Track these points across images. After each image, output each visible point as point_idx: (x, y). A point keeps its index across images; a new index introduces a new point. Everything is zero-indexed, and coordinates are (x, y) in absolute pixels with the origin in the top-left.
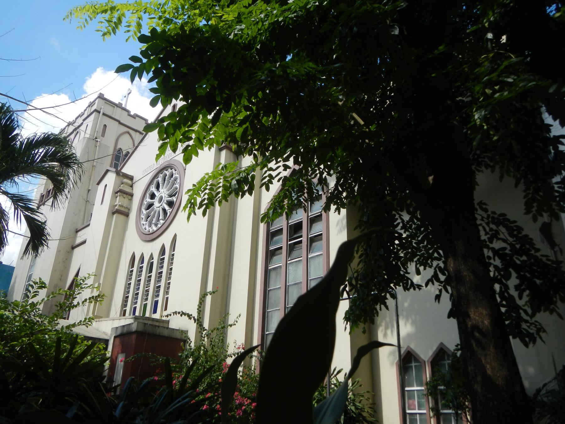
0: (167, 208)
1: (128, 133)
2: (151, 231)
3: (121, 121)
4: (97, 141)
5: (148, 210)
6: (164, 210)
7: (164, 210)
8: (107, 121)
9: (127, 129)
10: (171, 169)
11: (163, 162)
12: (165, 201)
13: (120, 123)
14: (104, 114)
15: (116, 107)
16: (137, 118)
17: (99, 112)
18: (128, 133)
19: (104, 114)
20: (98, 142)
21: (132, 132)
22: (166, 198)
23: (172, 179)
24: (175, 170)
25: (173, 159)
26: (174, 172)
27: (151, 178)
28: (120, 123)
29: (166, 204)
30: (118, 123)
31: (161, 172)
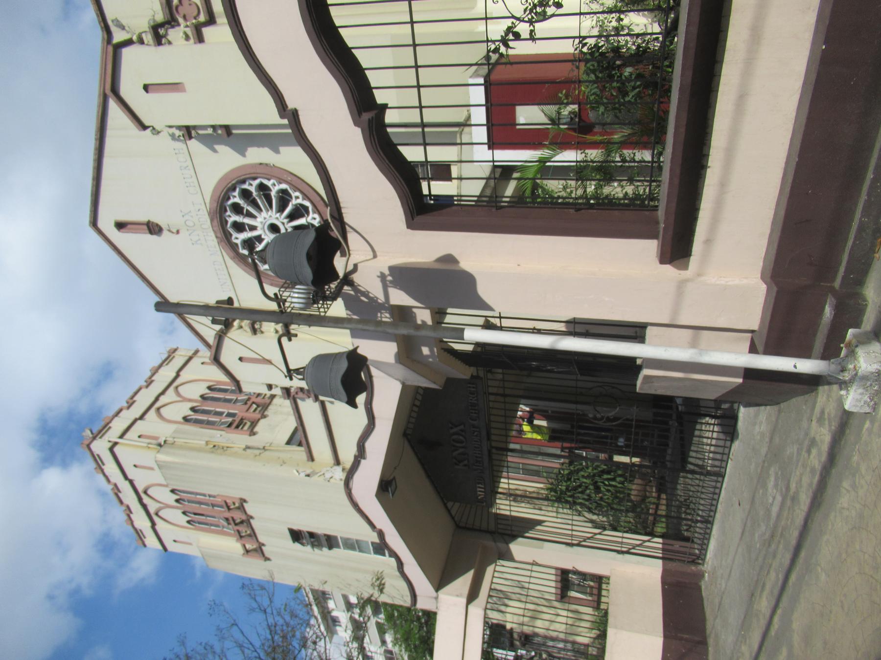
3: (138, 416)
4: (165, 441)
6: (292, 217)
7: (292, 217)
8: (132, 434)
12: (278, 215)
13: (141, 417)
14: (121, 437)
15: (110, 425)
16: (135, 399)
17: (116, 444)
20: (167, 439)
21: (158, 405)
28: (141, 417)
30: (139, 422)
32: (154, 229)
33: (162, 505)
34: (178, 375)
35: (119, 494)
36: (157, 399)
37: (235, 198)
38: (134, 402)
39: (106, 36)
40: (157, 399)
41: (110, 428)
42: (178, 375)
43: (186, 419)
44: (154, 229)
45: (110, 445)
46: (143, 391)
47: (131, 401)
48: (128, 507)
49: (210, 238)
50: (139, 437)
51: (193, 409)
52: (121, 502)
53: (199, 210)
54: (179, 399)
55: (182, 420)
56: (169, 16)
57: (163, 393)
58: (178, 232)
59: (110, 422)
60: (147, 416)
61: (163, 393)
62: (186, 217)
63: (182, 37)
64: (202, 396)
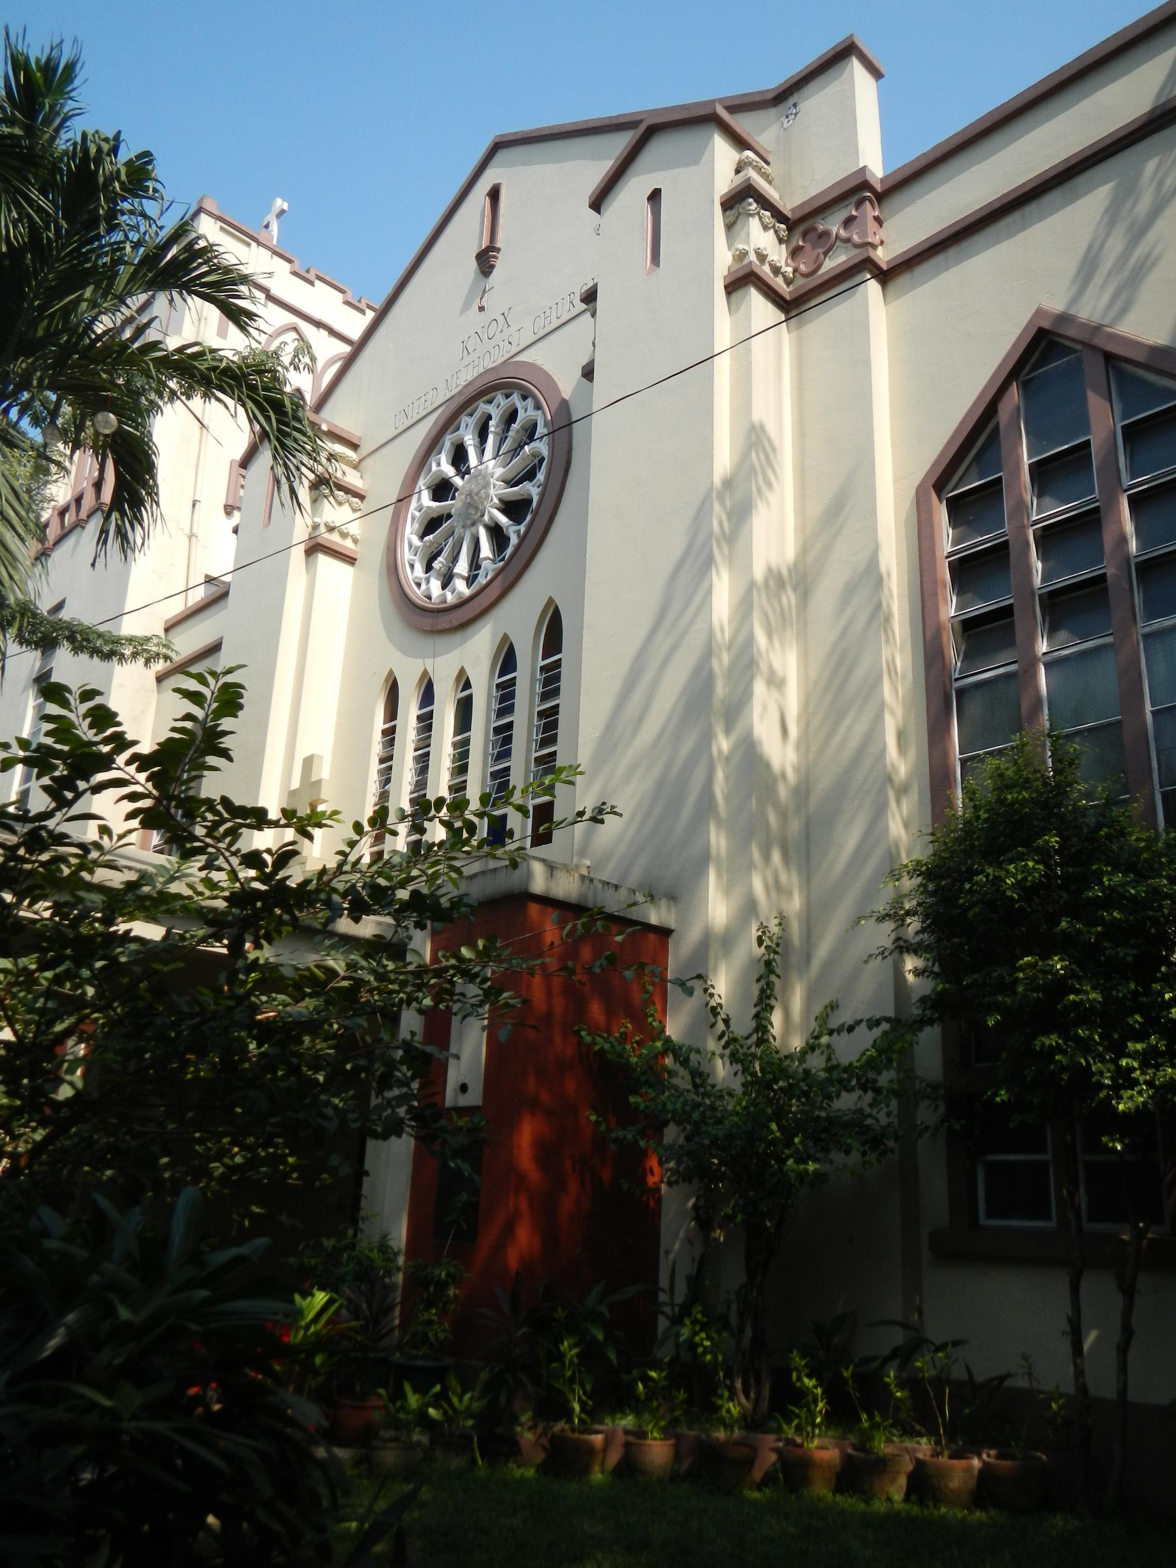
0: (503, 519)
1: (295, 329)
2: (450, 598)
3: (275, 292)
5: (431, 536)
6: (496, 532)
9: (292, 319)
10: (507, 396)
11: (475, 375)
12: (496, 501)
15: (254, 244)
18: (295, 329)
21: (305, 327)
22: (497, 491)
23: (515, 426)
24: (524, 398)
25: (518, 359)
26: (519, 404)
27: (434, 433)
29: (498, 509)
31: (468, 411)
32: (486, 260)
36: (318, 324)
37: (496, 410)
38: (312, 283)
39: (770, 96)
40: (318, 324)
41: (249, 245)
44: (486, 260)
46: (339, 296)
47: (311, 276)
49: (466, 375)
53: (510, 343)
56: (798, 215)
57: (333, 332)
58: (481, 309)
59: (259, 243)
61: (333, 332)
62: (501, 319)
63: (765, 249)
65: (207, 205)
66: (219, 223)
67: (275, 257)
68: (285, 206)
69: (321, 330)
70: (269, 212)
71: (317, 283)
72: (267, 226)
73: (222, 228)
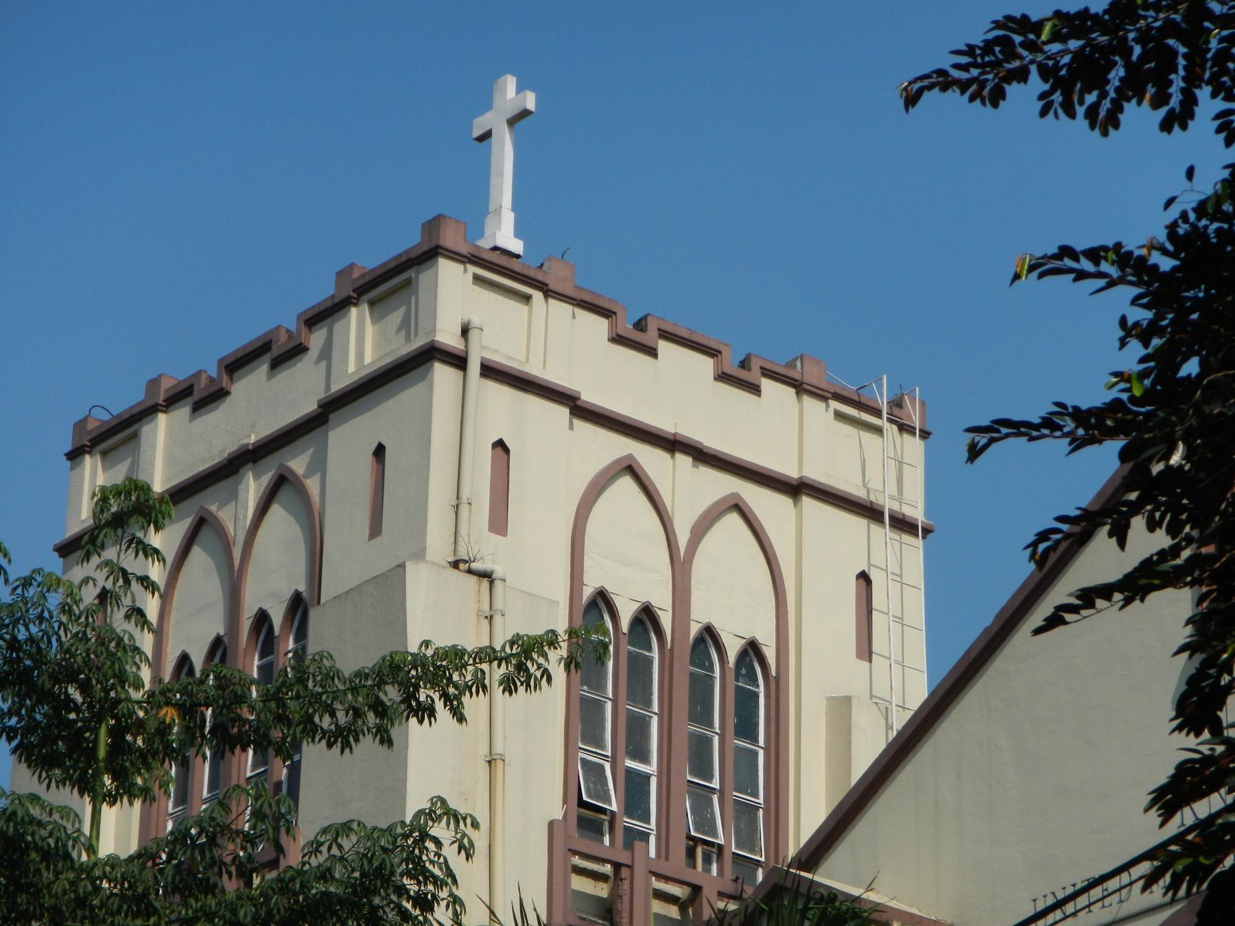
3: (590, 396)
14: (490, 371)
15: (537, 296)
17: (459, 361)
19: (490, 371)
21: (651, 459)
30: (564, 412)
33: (237, 553)
34: (795, 489)
35: (267, 358)
36: (672, 444)
38: (652, 352)
40: (672, 444)
41: (527, 299)
42: (795, 489)
43: (602, 601)
45: (448, 337)
48: (217, 395)
50: (500, 445)
51: (646, 617)
52: (237, 365)
54: (683, 538)
55: (587, 592)
59: (548, 293)
60: (585, 429)
64: (709, 632)
65: (449, 239)
66: (472, 269)
67: (580, 313)
68: (531, 105)
69: (678, 456)
70: (487, 105)
71: (664, 347)
72: (487, 135)
73: (477, 279)
